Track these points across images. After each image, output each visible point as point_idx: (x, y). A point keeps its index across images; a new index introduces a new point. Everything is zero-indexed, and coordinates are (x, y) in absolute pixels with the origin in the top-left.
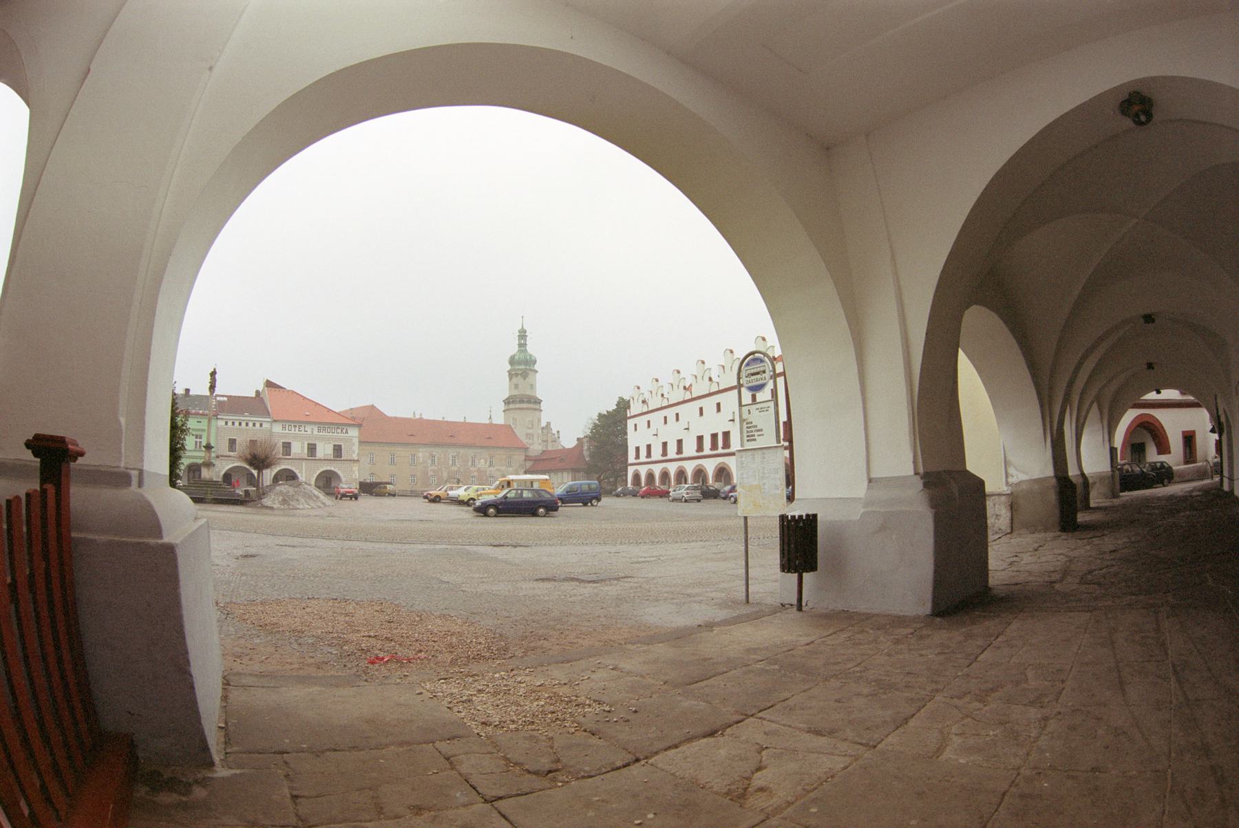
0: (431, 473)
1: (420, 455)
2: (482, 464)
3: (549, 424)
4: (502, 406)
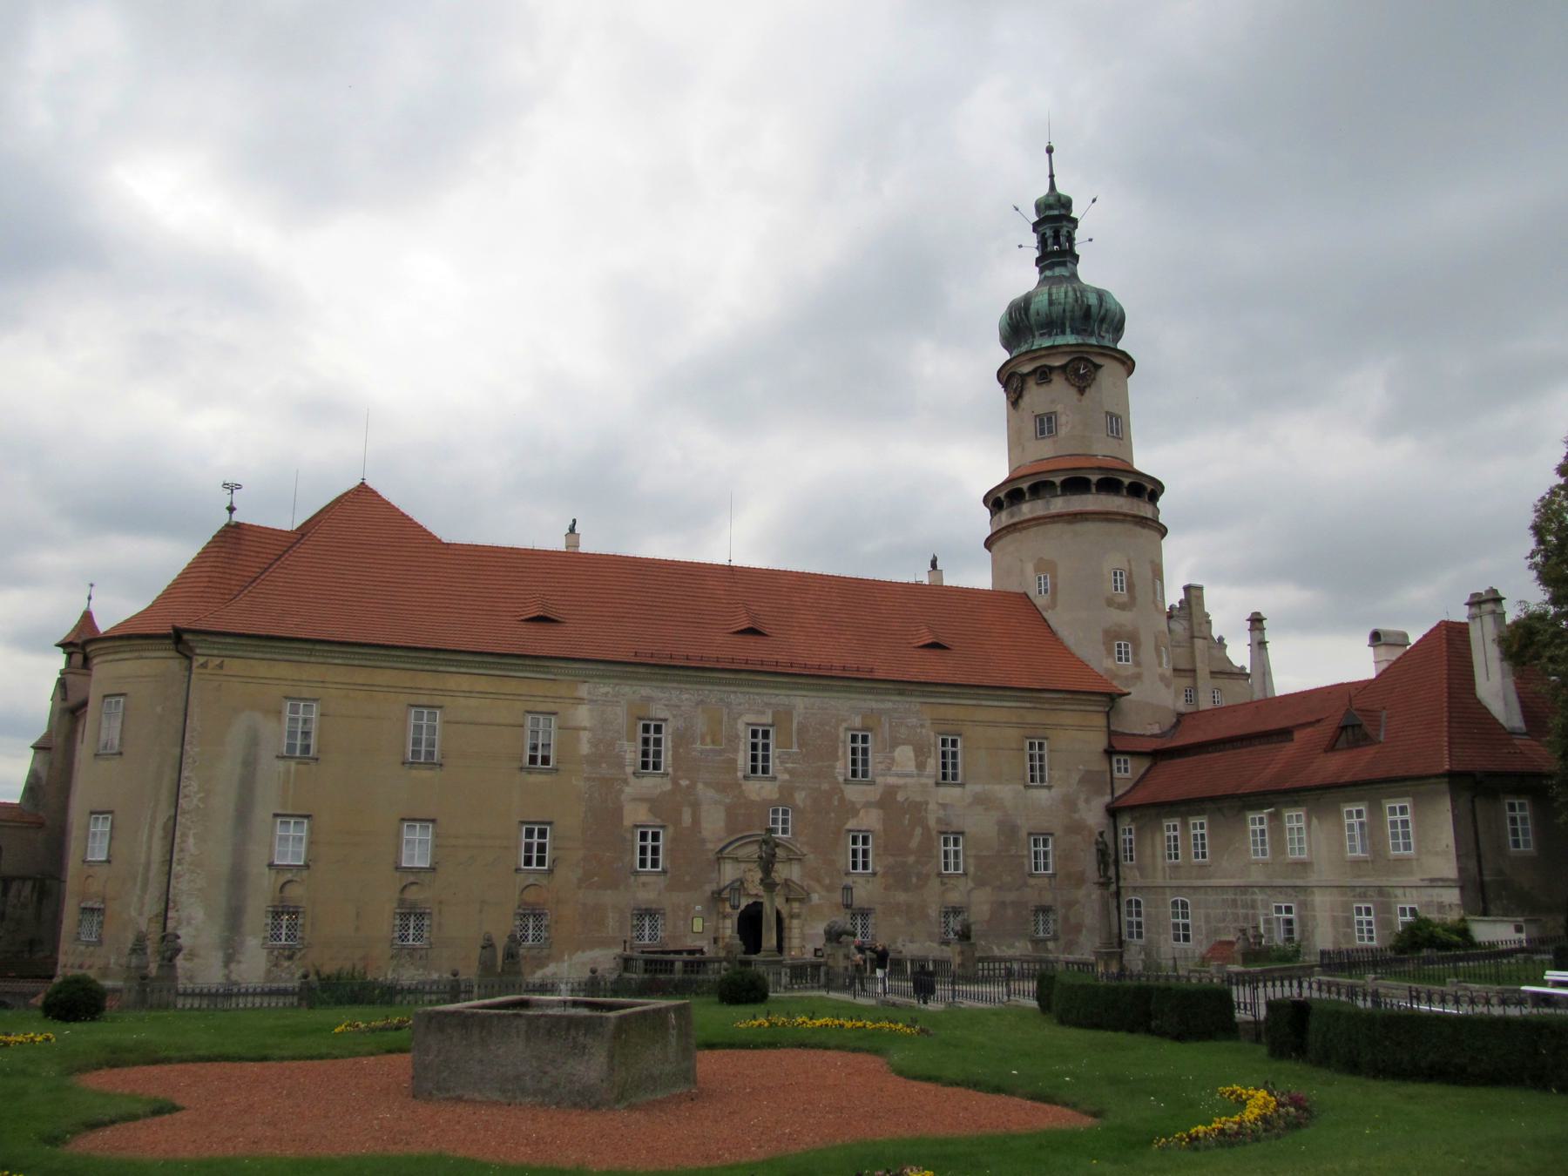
0: (637, 814)
1: (583, 715)
2: (902, 766)
3: (1193, 593)
4: (982, 521)
